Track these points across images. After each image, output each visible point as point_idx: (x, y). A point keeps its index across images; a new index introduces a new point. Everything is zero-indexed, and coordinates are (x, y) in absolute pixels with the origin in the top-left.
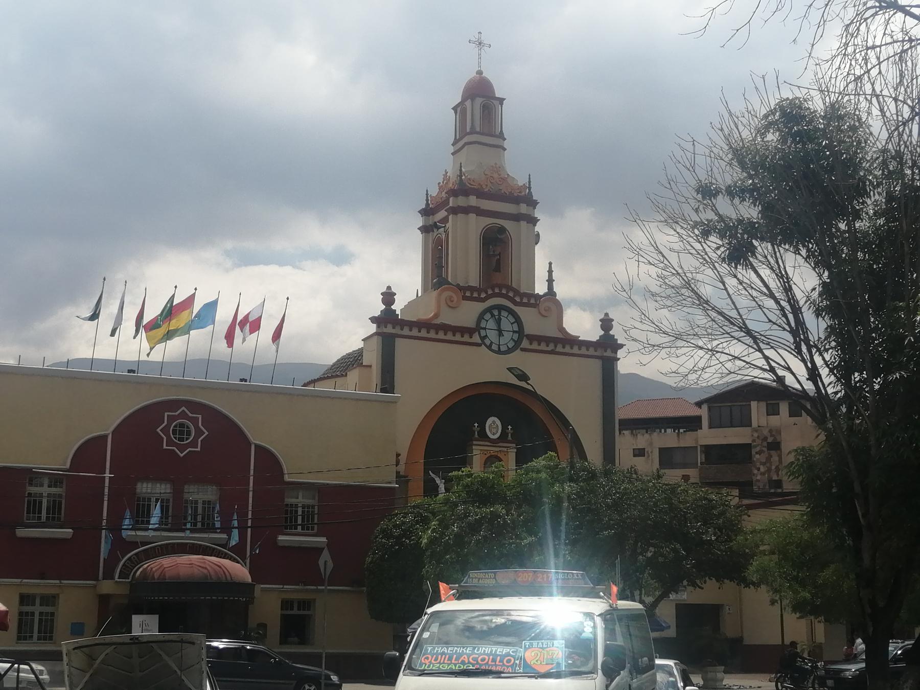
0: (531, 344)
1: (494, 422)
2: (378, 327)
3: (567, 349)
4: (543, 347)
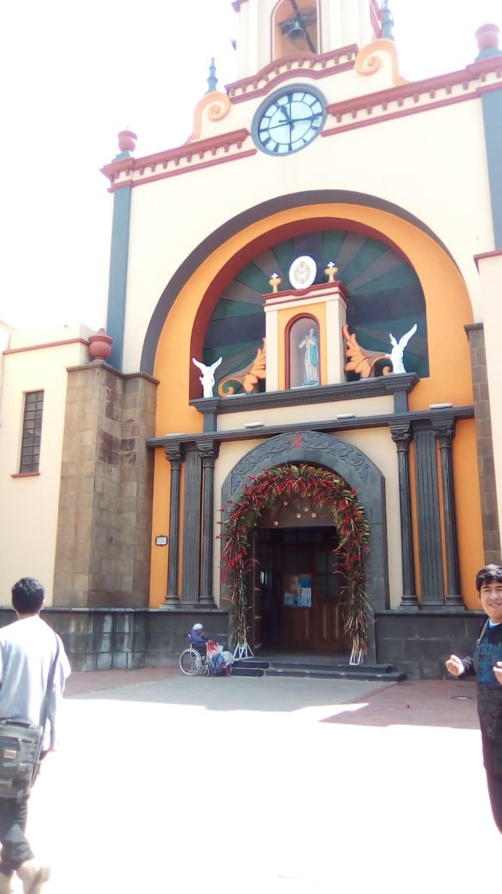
0: (339, 120)
1: (302, 264)
2: (112, 181)
3: (409, 103)
4: (362, 115)
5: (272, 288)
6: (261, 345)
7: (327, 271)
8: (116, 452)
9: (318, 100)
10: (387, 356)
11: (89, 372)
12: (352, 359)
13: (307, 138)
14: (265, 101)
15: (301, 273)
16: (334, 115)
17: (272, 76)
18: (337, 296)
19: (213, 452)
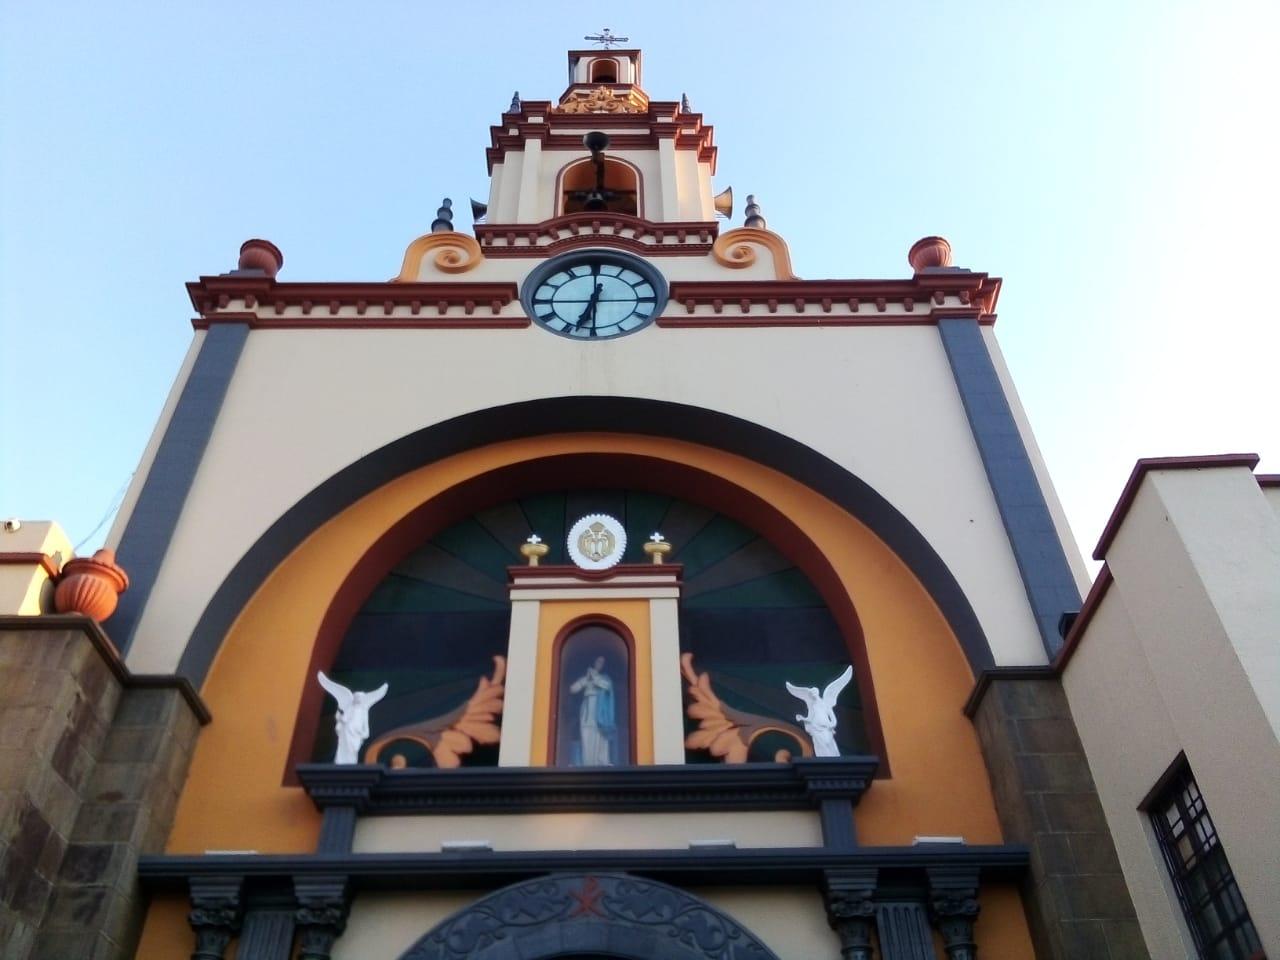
0: (691, 311)
1: (597, 527)
5: (526, 559)
6: (489, 670)
7: (648, 547)
8: (43, 877)
9: (646, 280)
10: (799, 718)
11: (45, 635)
12: (704, 724)
13: (626, 326)
14: (545, 264)
15: (596, 542)
16: (682, 300)
17: (564, 235)
18: (675, 592)
19: (337, 913)
